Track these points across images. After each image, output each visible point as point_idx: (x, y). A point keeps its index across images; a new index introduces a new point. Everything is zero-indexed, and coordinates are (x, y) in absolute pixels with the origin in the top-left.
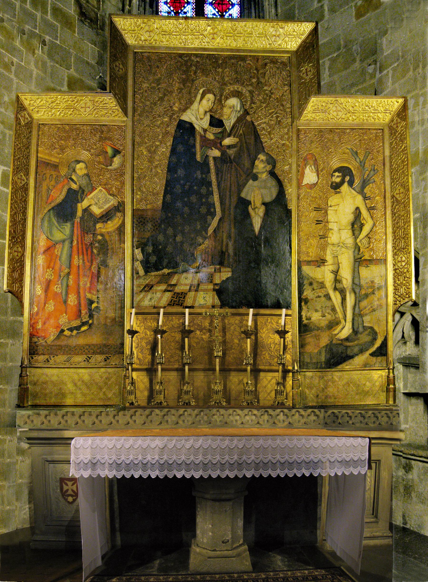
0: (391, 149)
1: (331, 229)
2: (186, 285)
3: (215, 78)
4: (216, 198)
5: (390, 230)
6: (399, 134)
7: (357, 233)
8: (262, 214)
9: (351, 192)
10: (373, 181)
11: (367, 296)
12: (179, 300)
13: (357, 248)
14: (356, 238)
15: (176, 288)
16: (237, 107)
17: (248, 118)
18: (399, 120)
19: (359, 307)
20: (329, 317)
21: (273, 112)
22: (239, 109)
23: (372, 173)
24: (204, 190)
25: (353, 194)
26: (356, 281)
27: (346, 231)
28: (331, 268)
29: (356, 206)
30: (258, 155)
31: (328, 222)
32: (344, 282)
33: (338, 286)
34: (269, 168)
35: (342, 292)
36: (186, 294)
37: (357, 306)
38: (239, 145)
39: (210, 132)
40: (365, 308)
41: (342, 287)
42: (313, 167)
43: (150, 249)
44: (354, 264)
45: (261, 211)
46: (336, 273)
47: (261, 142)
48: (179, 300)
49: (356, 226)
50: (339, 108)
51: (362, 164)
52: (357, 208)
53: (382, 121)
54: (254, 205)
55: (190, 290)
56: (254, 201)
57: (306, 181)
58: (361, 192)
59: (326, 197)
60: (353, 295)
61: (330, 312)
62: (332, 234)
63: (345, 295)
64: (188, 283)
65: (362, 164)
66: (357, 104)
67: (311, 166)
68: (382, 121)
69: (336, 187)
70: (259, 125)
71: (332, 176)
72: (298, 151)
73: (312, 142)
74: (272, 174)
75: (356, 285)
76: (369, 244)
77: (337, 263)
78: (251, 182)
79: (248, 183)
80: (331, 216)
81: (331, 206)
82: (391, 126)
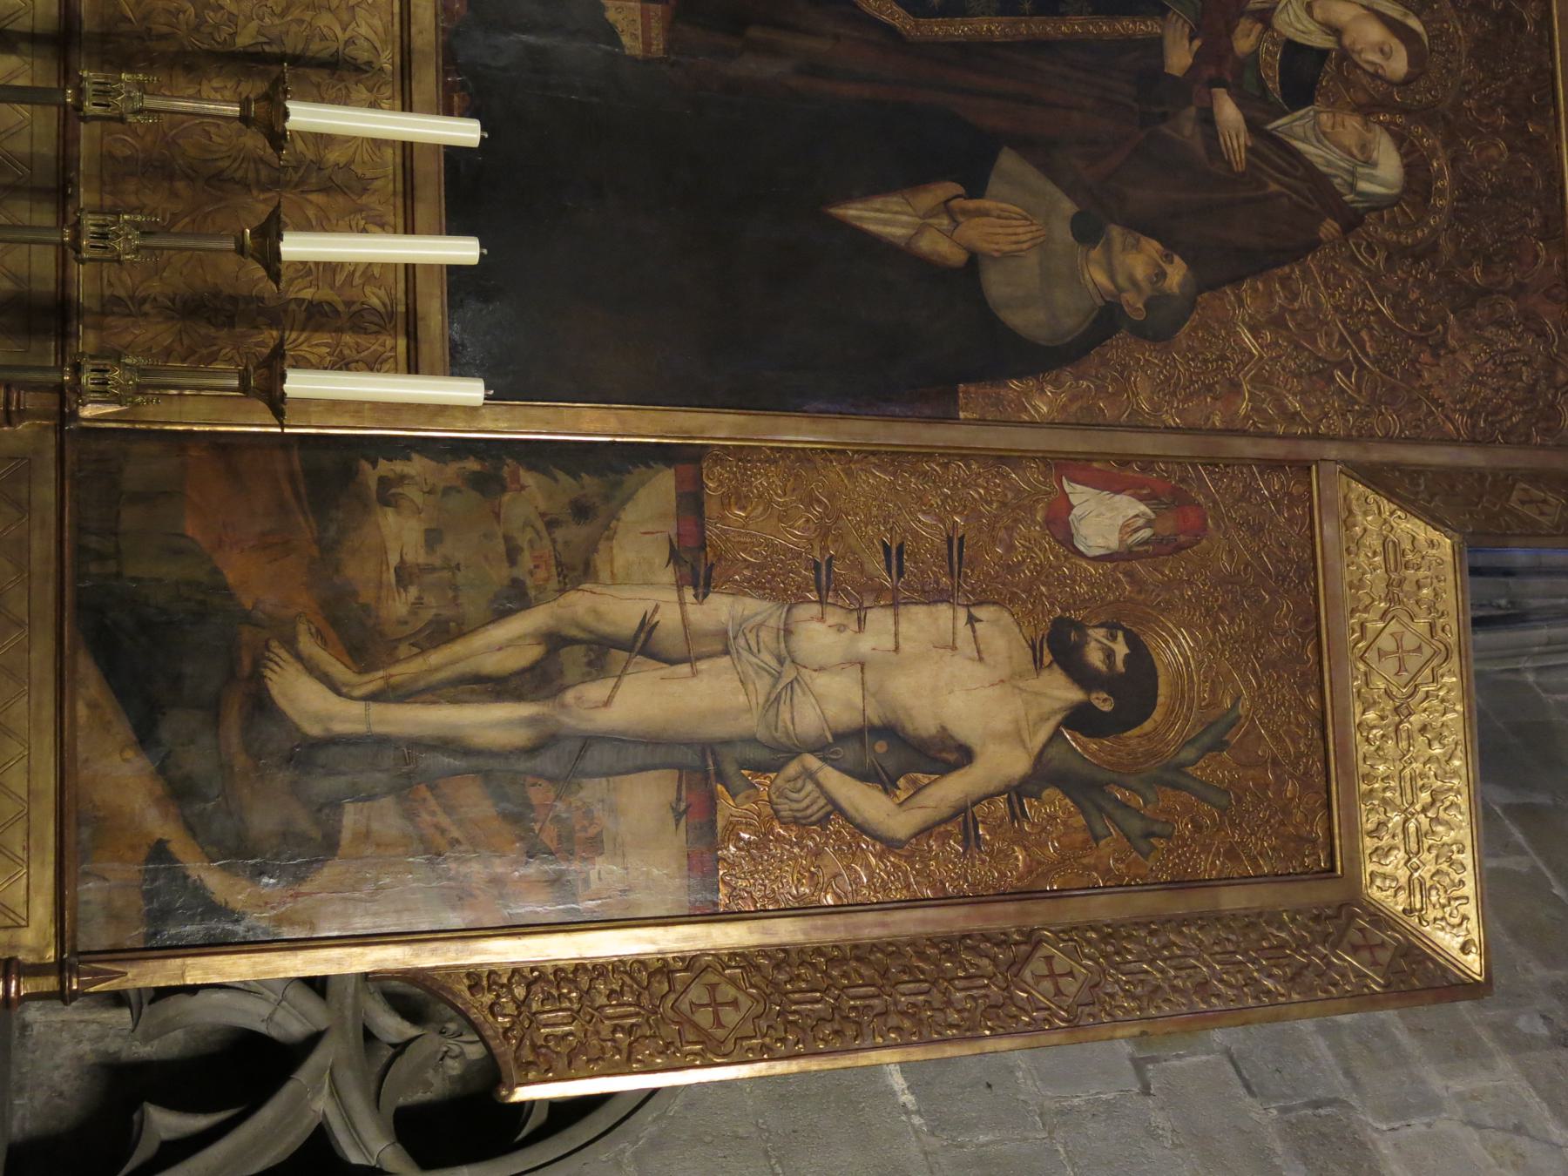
0: (1251, 921)
1: (861, 622)
3: (1469, 95)
5: (869, 928)
6: (1324, 958)
7: (849, 752)
9: (1044, 719)
10: (1099, 828)
11: (517, 816)
13: (775, 754)
14: (820, 749)
16: (1371, 179)
17: (1329, 228)
18: (1384, 956)
19: (456, 773)
20: (398, 606)
21: (1362, 348)
22: (1363, 186)
23: (1136, 826)
25: (1033, 734)
26: (599, 756)
27: (858, 700)
28: (669, 617)
29: (977, 749)
30: (1183, 258)
31: (895, 605)
32: (596, 691)
33: (573, 658)
34: (1134, 303)
35: (536, 681)
37: (457, 763)
39: (1260, 40)
40: (449, 810)
41: (569, 679)
42: (1146, 533)
44: (689, 744)
46: (644, 644)
47: (1236, 280)
49: (881, 747)
50: (1413, 662)
51: (1173, 776)
52: (965, 755)
53: (1370, 867)
56: (985, 213)
57: (1081, 497)
58: (1045, 774)
59: (1013, 598)
60: (520, 737)
61: (428, 615)
62: (841, 628)
63: (519, 697)
65: (1173, 776)
66: (1437, 750)
67: (1149, 523)
68: (1370, 867)
69: (1059, 647)
70: (1306, 273)
71: (1112, 628)
72: (1211, 463)
73: (1256, 530)
74: (1107, 320)
75: (575, 756)
76: (796, 821)
77: (696, 649)
78: (1068, 207)
79: (1058, 194)
80: (926, 622)
81: (972, 620)
82: (1354, 915)
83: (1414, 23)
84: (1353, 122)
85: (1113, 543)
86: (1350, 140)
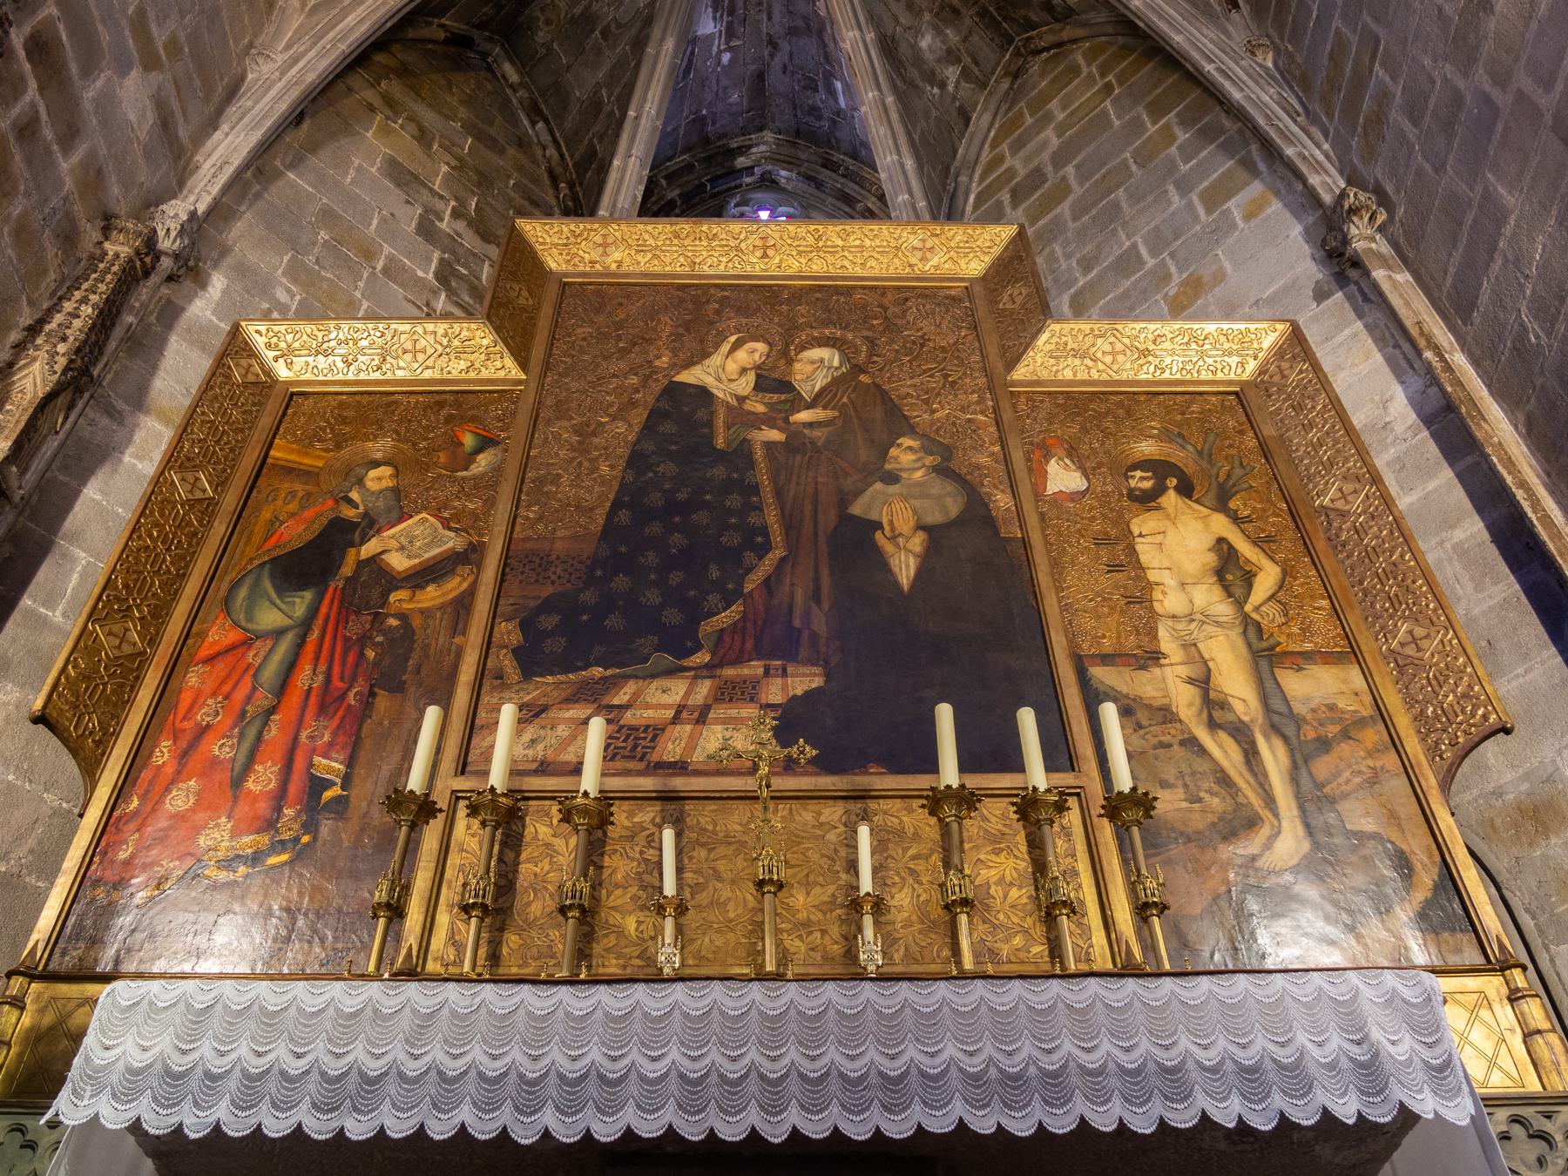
2: (665, 707)
4: (772, 517)
8: (918, 549)
12: (635, 747)
15: (629, 714)
22: (836, 363)
24: (734, 501)
36: (663, 730)
38: (839, 423)
43: (549, 622)
45: (918, 542)
47: (906, 418)
48: (635, 747)
54: (893, 530)
55: (676, 720)
56: (891, 523)
64: (670, 701)
74: (943, 471)
78: (878, 486)
83: (733, 339)
84: (797, 366)
85: (1078, 474)
86: (810, 368)
